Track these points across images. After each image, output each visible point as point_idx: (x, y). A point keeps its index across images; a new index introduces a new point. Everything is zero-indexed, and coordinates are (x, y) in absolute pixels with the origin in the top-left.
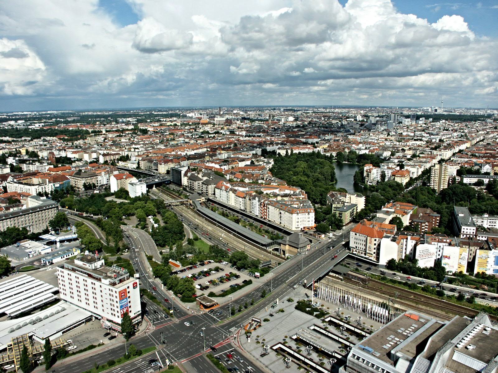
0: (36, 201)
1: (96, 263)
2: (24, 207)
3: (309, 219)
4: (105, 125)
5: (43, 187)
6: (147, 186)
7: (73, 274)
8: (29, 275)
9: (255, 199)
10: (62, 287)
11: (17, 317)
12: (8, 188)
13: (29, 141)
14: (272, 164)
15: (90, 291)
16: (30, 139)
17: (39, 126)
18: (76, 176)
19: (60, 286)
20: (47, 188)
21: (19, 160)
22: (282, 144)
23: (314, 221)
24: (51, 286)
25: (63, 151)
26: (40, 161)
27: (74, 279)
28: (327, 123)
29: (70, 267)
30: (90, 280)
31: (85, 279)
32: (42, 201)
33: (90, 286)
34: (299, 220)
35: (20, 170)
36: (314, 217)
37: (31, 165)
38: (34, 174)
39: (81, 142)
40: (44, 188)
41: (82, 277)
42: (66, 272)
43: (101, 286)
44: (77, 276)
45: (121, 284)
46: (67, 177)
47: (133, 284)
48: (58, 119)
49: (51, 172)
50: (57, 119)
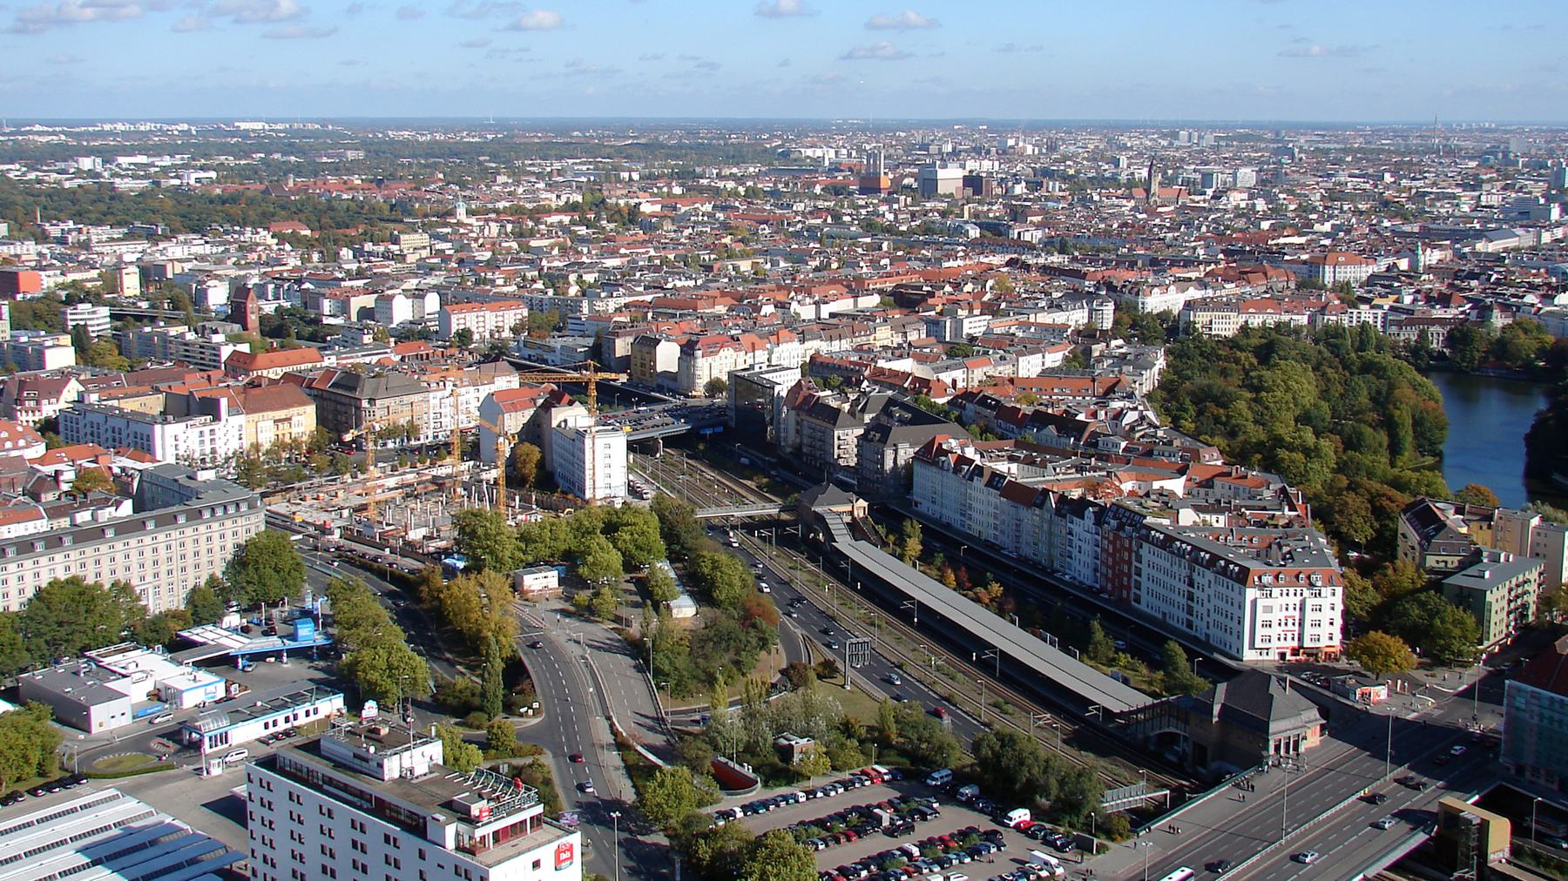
3: (1317, 616)
6: (632, 447)
9: (1082, 518)
14: (1156, 370)
22: (1200, 282)
23: (1339, 622)
27: (313, 820)
28: (1409, 199)
34: (1275, 617)
36: (1340, 607)
43: (422, 855)
45: (506, 847)
47: (558, 852)
48: (277, 156)
50: (269, 153)
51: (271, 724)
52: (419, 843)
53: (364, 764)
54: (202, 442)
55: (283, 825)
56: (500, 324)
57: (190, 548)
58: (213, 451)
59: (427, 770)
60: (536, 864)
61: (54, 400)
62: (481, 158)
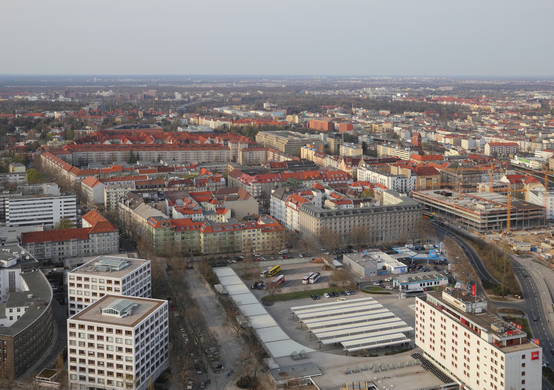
0: (394, 198)
1: (474, 304)
2: (377, 204)
4: (494, 100)
5: (404, 180)
7: (439, 314)
8: (375, 299)
10: (420, 329)
11: (355, 354)
12: (358, 175)
13: (387, 116)
15: (461, 346)
16: (389, 112)
17: (402, 96)
18: (450, 169)
19: (417, 326)
20: (408, 181)
21: (374, 140)
24: (404, 323)
25: (433, 133)
26: (402, 146)
27: (438, 322)
29: (436, 301)
30: (462, 330)
31: (456, 324)
32: (401, 198)
33: (461, 338)
35: (375, 153)
37: (389, 149)
38: (394, 160)
39: (457, 122)
40: (404, 181)
41: (450, 322)
42: (428, 307)
43: (478, 342)
44: (445, 317)
45: (511, 348)
46: (437, 169)
49: (416, 161)
51: (430, 284)
52: (478, 338)
53: (458, 305)
54: (402, 184)
55: (428, 322)
56: (508, 151)
57: (397, 219)
58: (406, 187)
59: (481, 311)
60: (524, 357)
61: (356, 166)
62: (501, 90)
